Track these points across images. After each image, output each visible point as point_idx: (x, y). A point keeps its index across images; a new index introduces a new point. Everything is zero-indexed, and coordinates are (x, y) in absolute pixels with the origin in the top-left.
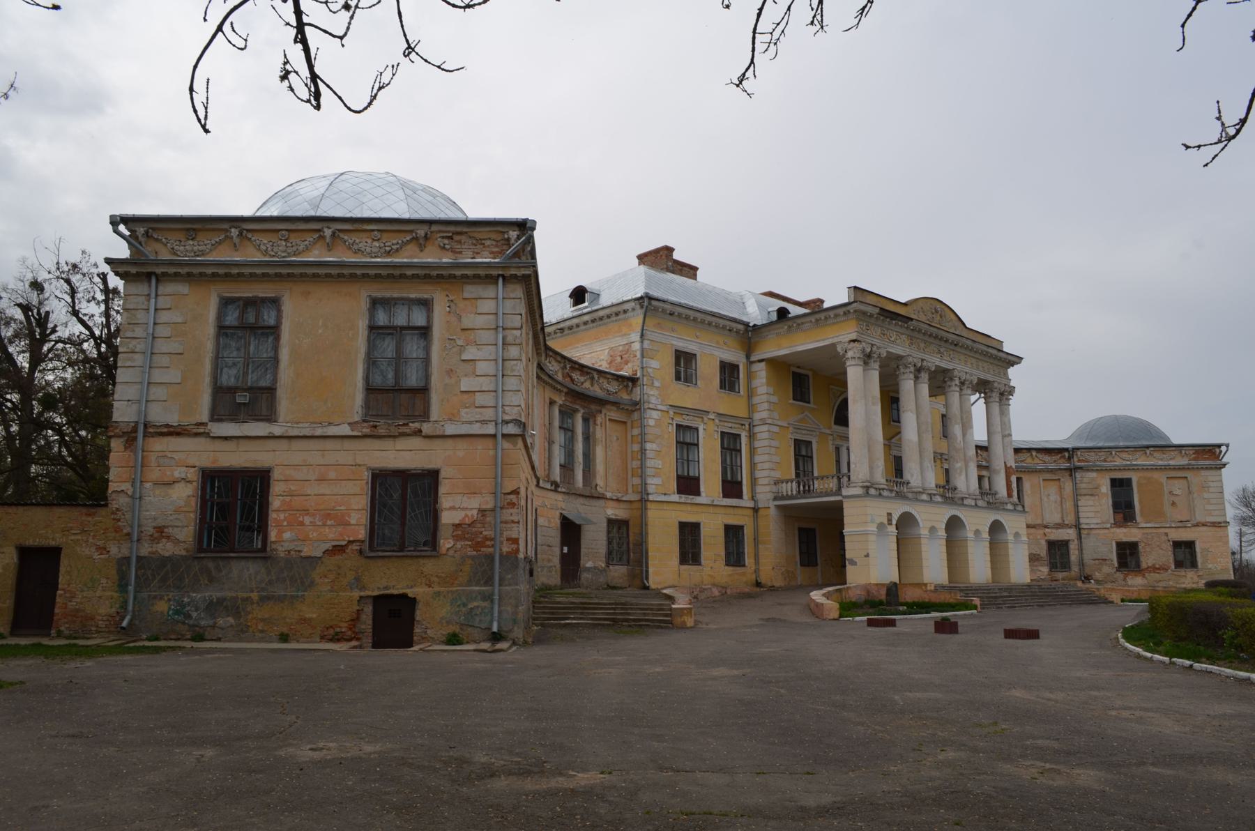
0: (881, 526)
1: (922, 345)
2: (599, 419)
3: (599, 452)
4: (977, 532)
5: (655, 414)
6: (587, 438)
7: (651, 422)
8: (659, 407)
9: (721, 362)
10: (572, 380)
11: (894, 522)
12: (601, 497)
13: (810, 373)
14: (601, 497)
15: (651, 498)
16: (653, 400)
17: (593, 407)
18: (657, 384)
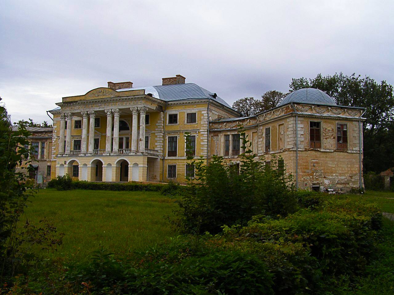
0: (62, 165)
1: (90, 106)
2: (46, 143)
3: (45, 150)
4: (110, 165)
5: (54, 139)
6: (43, 148)
7: (53, 142)
8: (55, 137)
9: (75, 121)
10: (36, 136)
11: (67, 163)
12: (46, 161)
13: (100, 117)
14: (46, 161)
15: (51, 160)
16: (54, 136)
17: (44, 141)
18: (56, 132)
